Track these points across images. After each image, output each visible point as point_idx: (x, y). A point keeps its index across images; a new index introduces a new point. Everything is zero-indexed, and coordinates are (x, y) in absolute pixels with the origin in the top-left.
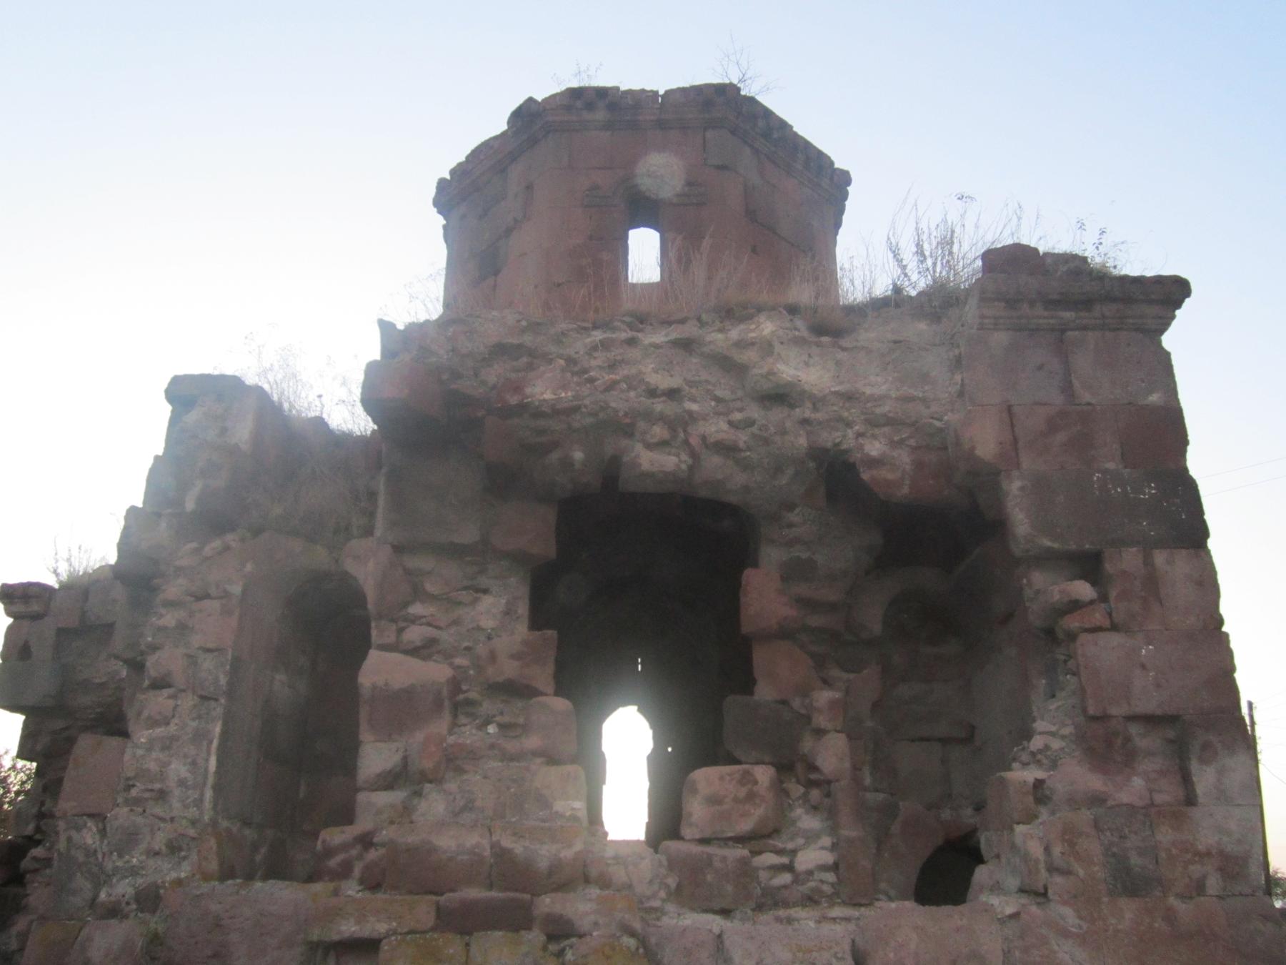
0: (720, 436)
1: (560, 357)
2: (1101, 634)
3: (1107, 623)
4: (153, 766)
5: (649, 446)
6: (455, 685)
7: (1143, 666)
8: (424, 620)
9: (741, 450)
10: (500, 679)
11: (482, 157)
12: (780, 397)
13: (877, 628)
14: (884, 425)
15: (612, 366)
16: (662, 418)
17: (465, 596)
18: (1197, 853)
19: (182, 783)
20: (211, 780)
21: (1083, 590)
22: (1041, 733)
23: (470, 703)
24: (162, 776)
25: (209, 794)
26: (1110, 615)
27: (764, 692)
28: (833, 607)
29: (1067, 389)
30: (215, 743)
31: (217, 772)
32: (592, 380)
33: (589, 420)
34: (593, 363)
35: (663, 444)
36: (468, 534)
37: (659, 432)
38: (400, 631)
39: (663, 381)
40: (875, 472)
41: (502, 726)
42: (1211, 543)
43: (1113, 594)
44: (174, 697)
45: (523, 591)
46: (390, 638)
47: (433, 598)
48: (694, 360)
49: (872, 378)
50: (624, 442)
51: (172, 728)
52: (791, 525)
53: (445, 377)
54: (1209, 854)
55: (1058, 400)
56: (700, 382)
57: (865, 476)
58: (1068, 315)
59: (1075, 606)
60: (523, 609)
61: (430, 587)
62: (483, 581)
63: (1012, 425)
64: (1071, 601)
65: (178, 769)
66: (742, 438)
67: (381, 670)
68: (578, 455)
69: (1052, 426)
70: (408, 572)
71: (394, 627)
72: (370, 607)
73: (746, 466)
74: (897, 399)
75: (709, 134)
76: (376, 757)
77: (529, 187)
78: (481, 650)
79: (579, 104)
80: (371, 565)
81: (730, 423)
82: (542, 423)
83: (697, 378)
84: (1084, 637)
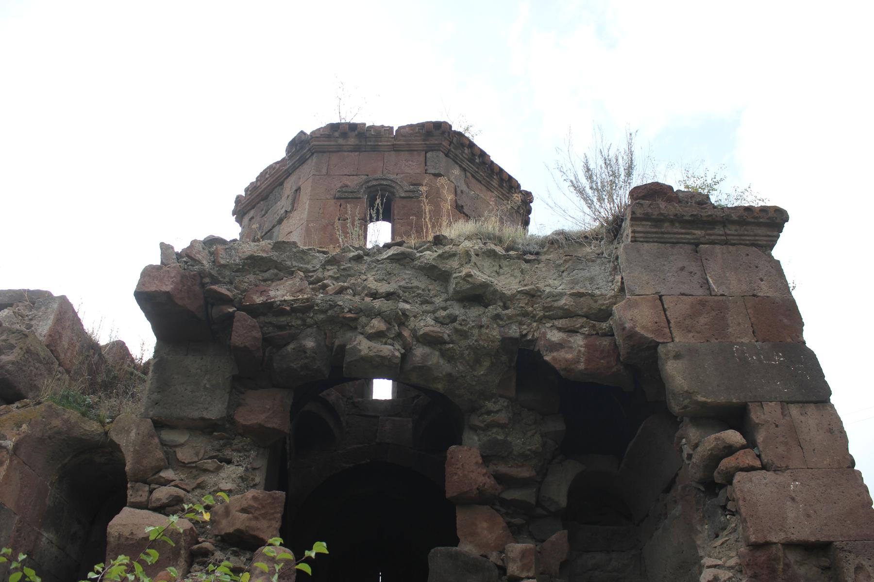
0: (427, 329)
1: (300, 269)
2: (754, 473)
3: (758, 463)
5: (370, 337)
6: (193, 536)
7: (793, 499)
8: (173, 483)
9: (445, 343)
11: (267, 176)
12: (477, 296)
13: (563, 502)
14: (561, 318)
16: (379, 314)
17: (210, 464)
21: (734, 436)
22: (709, 567)
26: (759, 456)
27: (466, 547)
28: (524, 483)
32: (325, 287)
33: (321, 317)
34: (327, 274)
36: (215, 411)
37: (377, 324)
38: (151, 492)
39: (383, 288)
40: (555, 354)
42: (833, 399)
43: (760, 438)
45: (261, 463)
46: (144, 499)
47: (184, 466)
48: (408, 272)
50: (349, 334)
52: (489, 413)
53: (207, 280)
56: (412, 288)
57: (547, 358)
59: (730, 450)
60: (259, 478)
62: (228, 453)
63: (665, 310)
64: (725, 447)
66: (446, 332)
67: (127, 521)
68: (310, 344)
70: (163, 443)
71: (147, 488)
72: (127, 468)
73: (449, 356)
74: (572, 295)
77: (298, 190)
79: (337, 134)
80: (133, 434)
81: (436, 320)
82: (283, 320)
83: (410, 285)
84: (738, 477)
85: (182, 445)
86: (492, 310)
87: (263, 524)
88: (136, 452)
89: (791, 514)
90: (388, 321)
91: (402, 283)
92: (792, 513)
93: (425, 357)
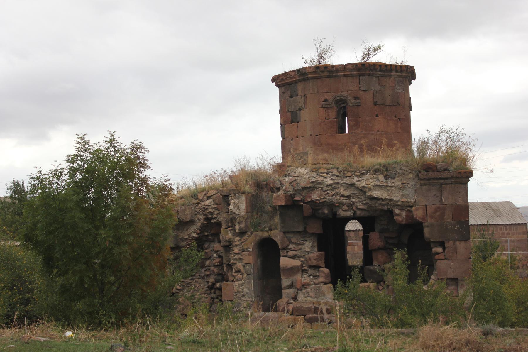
4: (240, 290)
5: (343, 211)
6: (302, 266)
10: (312, 265)
15: (334, 189)
19: (247, 293)
21: (440, 250)
23: (305, 270)
24: (243, 292)
25: (253, 295)
29: (441, 201)
35: (346, 211)
36: (301, 229)
38: (287, 252)
39: (346, 193)
41: (314, 276)
43: (446, 251)
44: (242, 274)
46: (285, 254)
47: (294, 243)
49: (396, 194)
51: (243, 281)
55: (438, 204)
58: (442, 181)
59: (438, 253)
60: (316, 244)
61: (293, 241)
67: (284, 262)
69: (436, 211)
75: (361, 78)
76: (285, 282)
77: (305, 95)
78: (307, 256)
79: (319, 71)
86: (378, 202)
87: (320, 262)
90: (348, 206)
91: (352, 192)
93: (360, 214)
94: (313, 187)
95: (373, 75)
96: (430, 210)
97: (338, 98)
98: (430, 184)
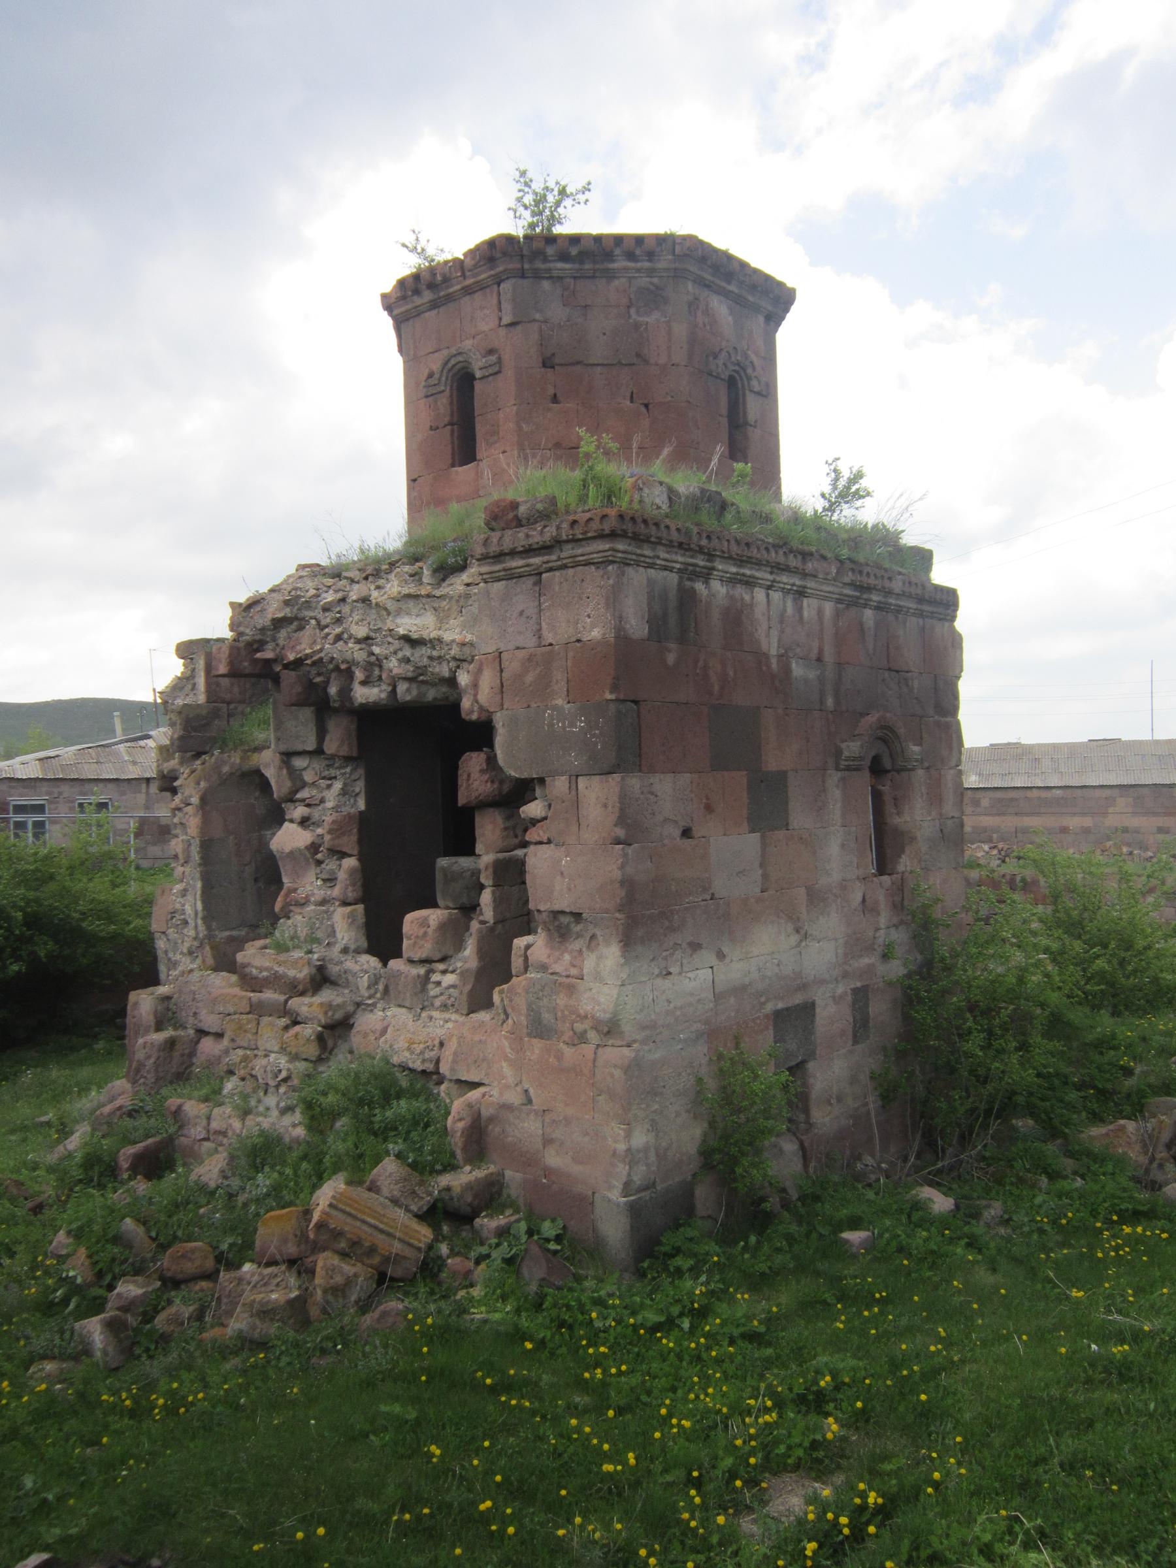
4: (178, 906)
6: (314, 848)
18: (579, 1016)
20: (200, 915)
24: (183, 912)
25: (200, 922)
29: (538, 634)
30: (199, 893)
31: (205, 908)
45: (361, 772)
54: (586, 1017)
55: (531, 642)
58: (536, 560)
60: (360, 786)
62: (333, 772)
65: (188, 909)
85: (305, 769)
87: (345, 838)
88: (277, 782)
89: (557, 888)
92: (560, 885)
94: (296, 618)
95: (537, 276)
96: (512, 666)
97: (453, 362)
98: (511, 576)
